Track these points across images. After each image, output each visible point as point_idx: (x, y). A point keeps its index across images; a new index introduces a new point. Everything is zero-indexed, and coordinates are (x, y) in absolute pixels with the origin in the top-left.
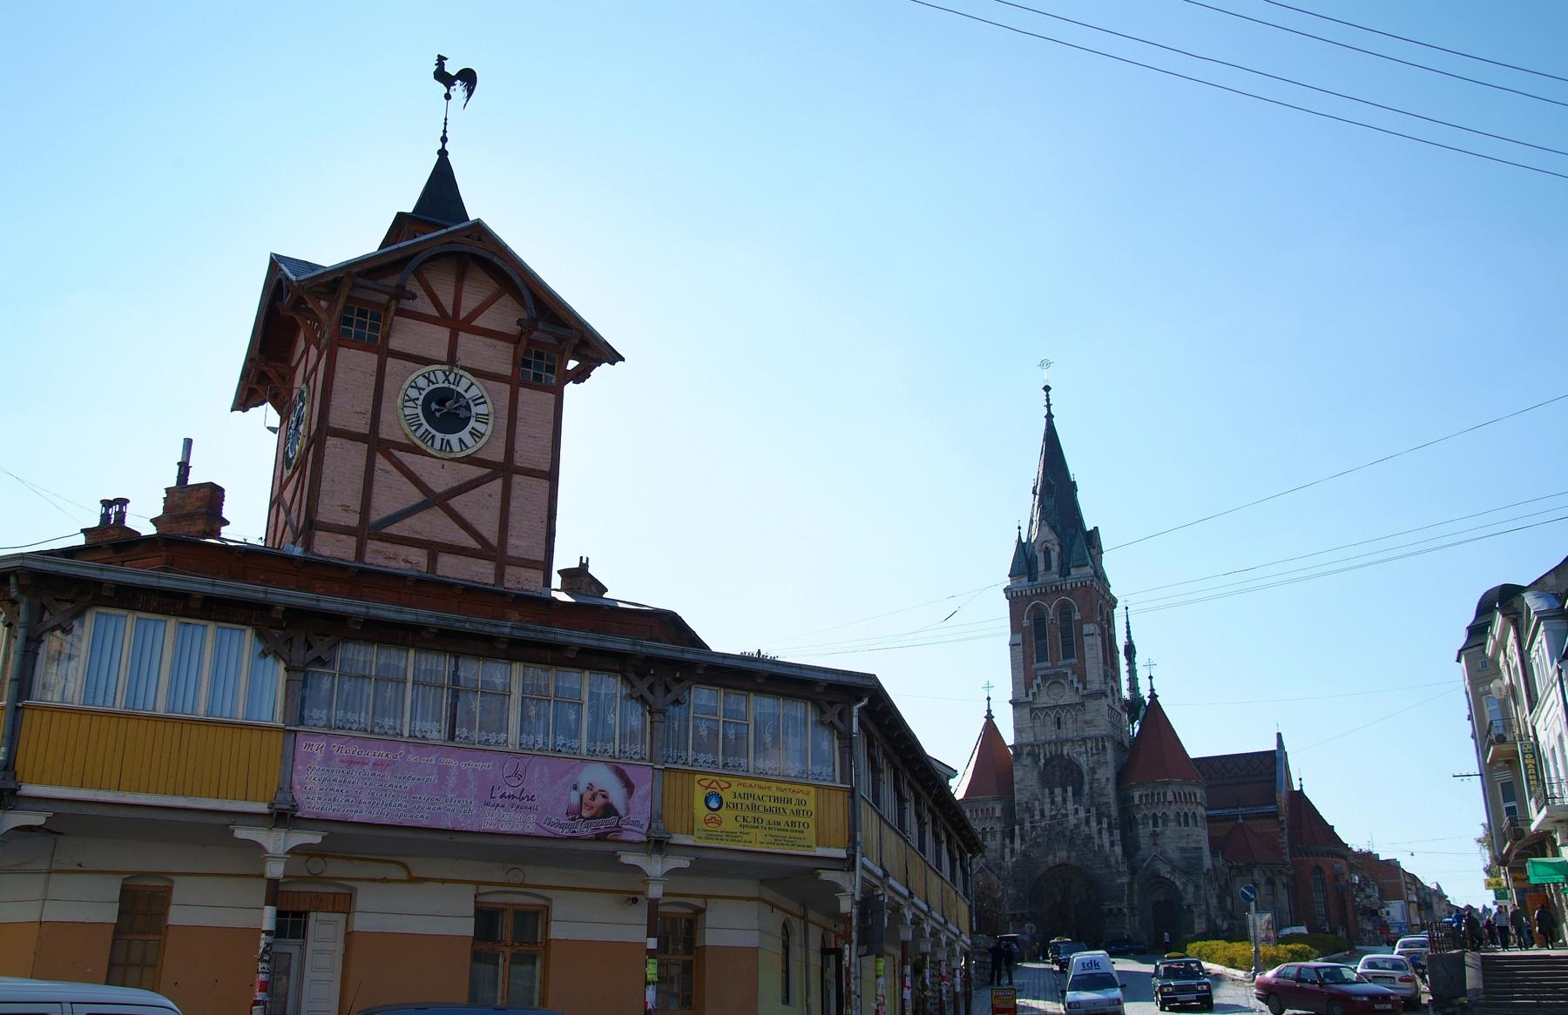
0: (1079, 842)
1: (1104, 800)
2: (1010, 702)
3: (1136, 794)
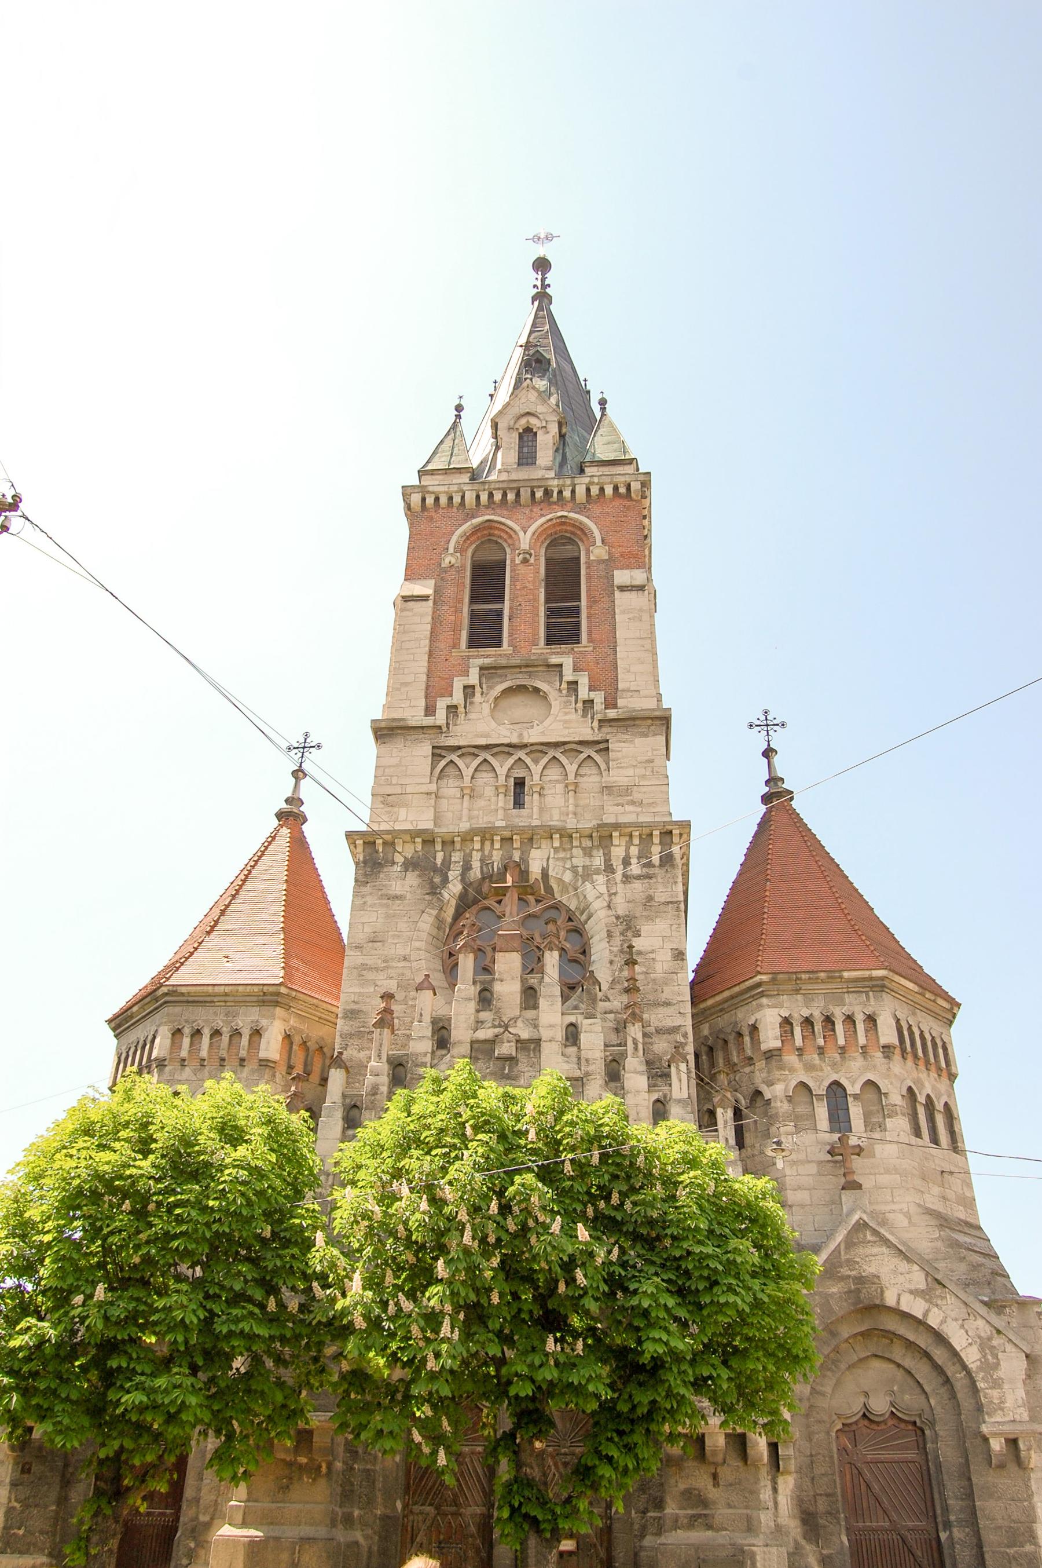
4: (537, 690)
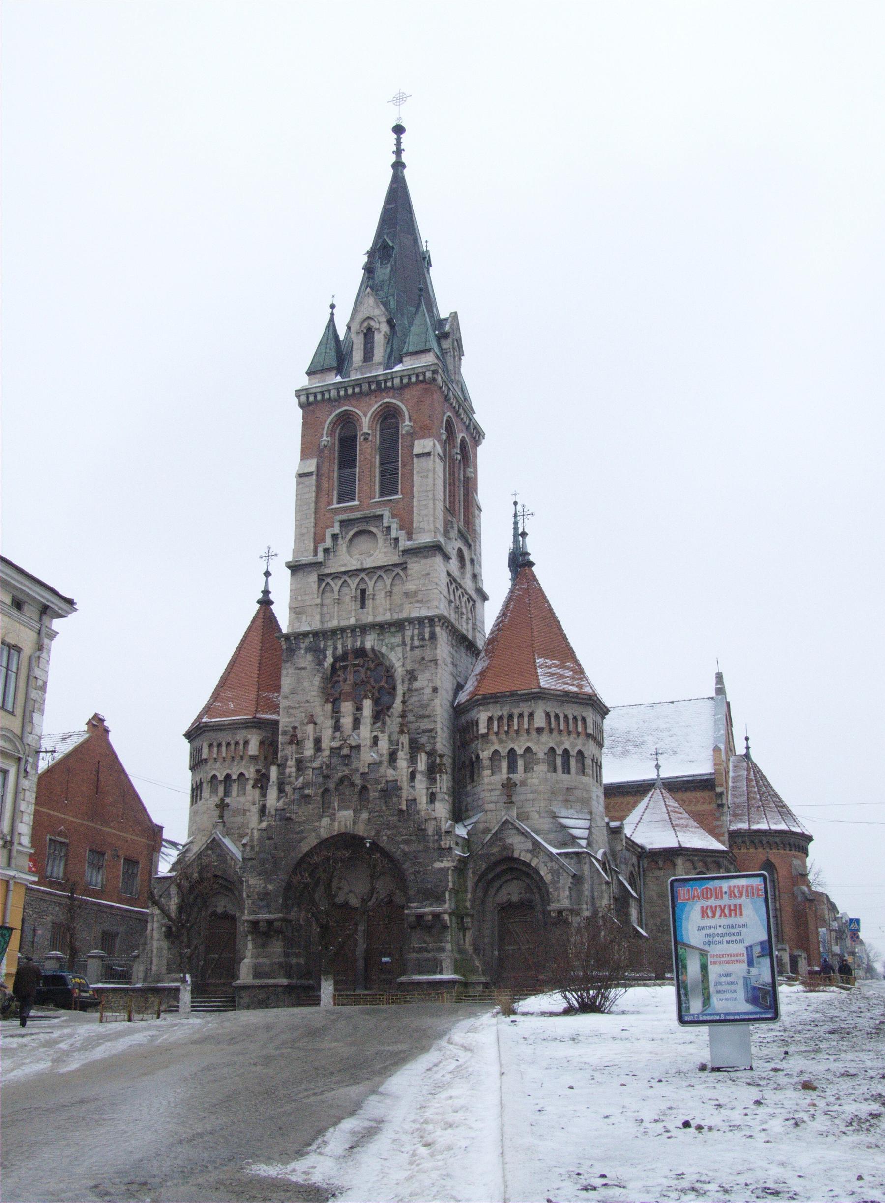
0: (373, 795)
1: (425, 724)
3: (483, 716)
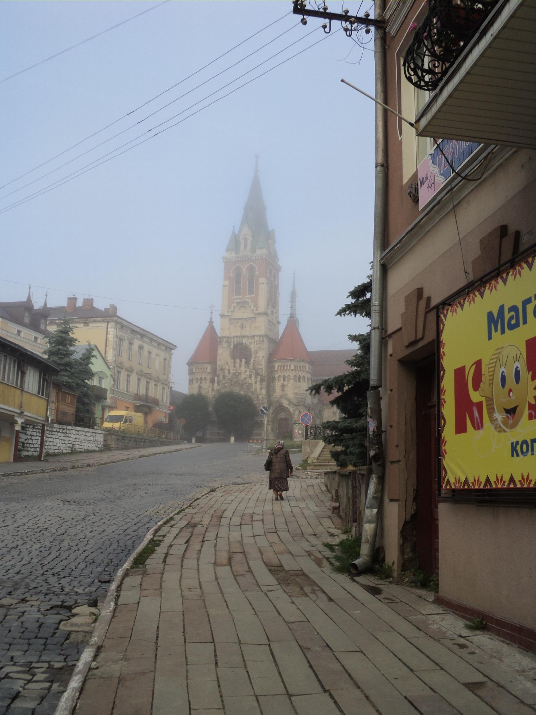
0: (245, 387)
1: (260, 367)
2: (220, 315)
3: (276, 365)
4: (245, 307)
